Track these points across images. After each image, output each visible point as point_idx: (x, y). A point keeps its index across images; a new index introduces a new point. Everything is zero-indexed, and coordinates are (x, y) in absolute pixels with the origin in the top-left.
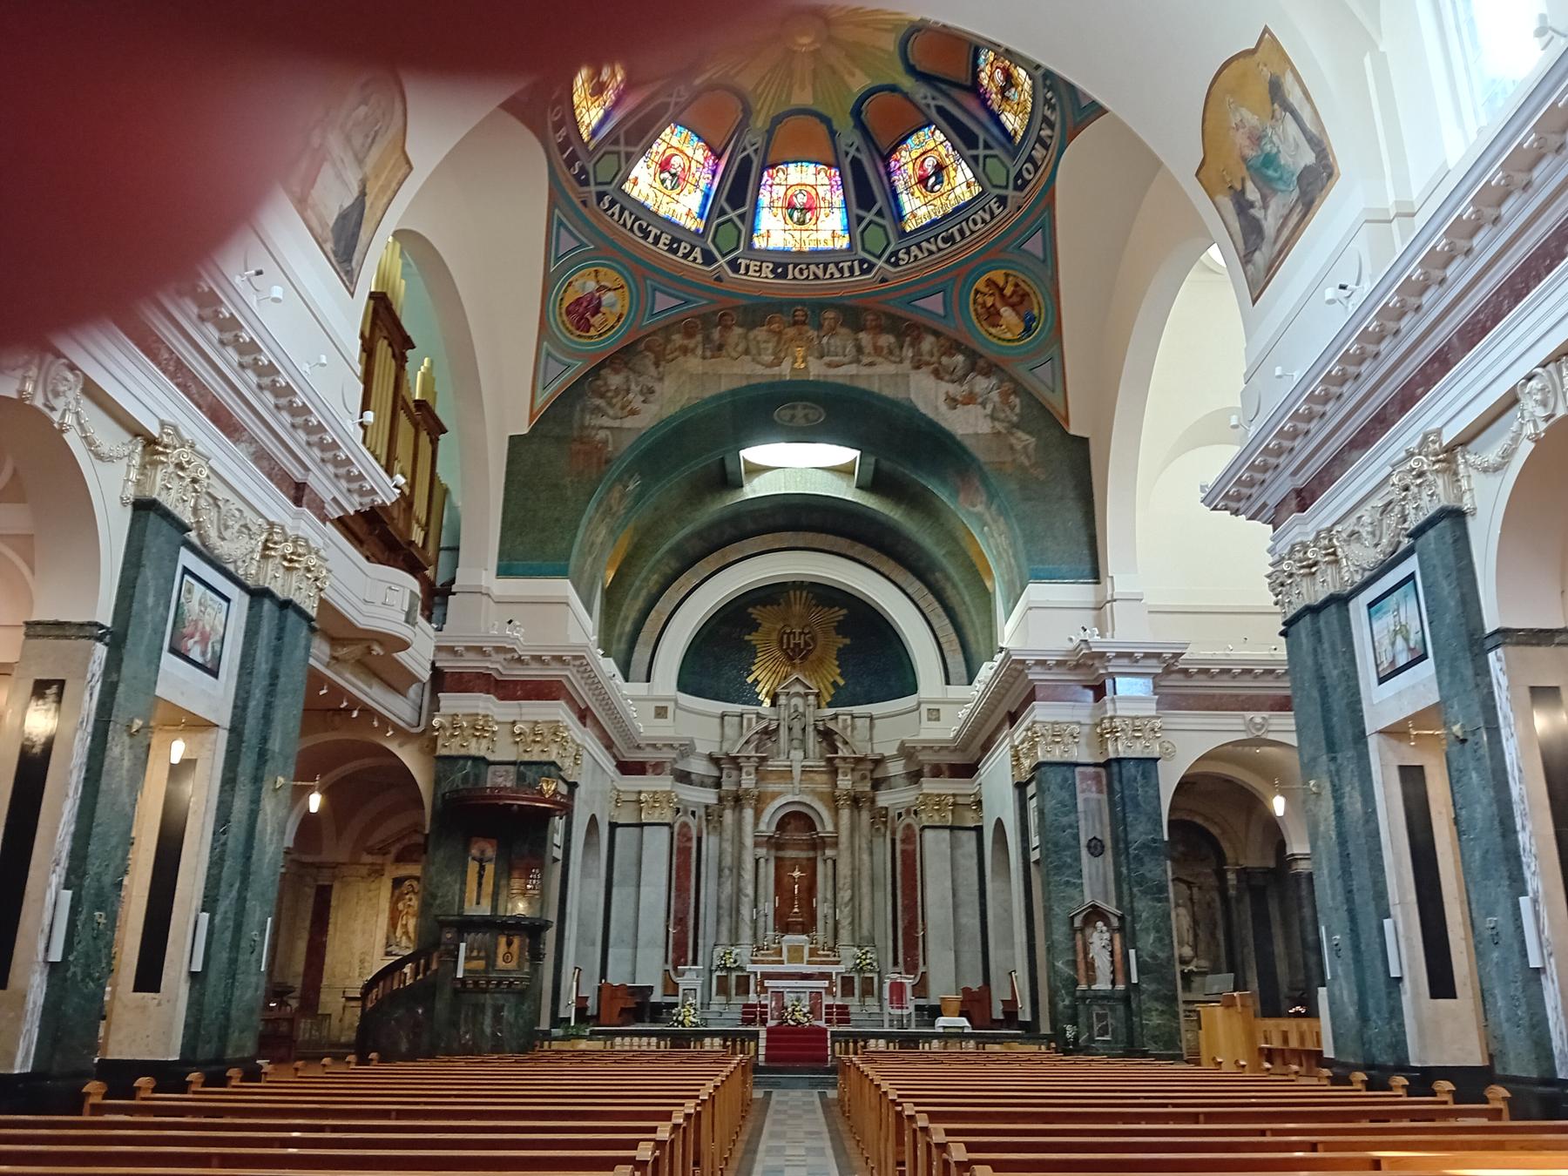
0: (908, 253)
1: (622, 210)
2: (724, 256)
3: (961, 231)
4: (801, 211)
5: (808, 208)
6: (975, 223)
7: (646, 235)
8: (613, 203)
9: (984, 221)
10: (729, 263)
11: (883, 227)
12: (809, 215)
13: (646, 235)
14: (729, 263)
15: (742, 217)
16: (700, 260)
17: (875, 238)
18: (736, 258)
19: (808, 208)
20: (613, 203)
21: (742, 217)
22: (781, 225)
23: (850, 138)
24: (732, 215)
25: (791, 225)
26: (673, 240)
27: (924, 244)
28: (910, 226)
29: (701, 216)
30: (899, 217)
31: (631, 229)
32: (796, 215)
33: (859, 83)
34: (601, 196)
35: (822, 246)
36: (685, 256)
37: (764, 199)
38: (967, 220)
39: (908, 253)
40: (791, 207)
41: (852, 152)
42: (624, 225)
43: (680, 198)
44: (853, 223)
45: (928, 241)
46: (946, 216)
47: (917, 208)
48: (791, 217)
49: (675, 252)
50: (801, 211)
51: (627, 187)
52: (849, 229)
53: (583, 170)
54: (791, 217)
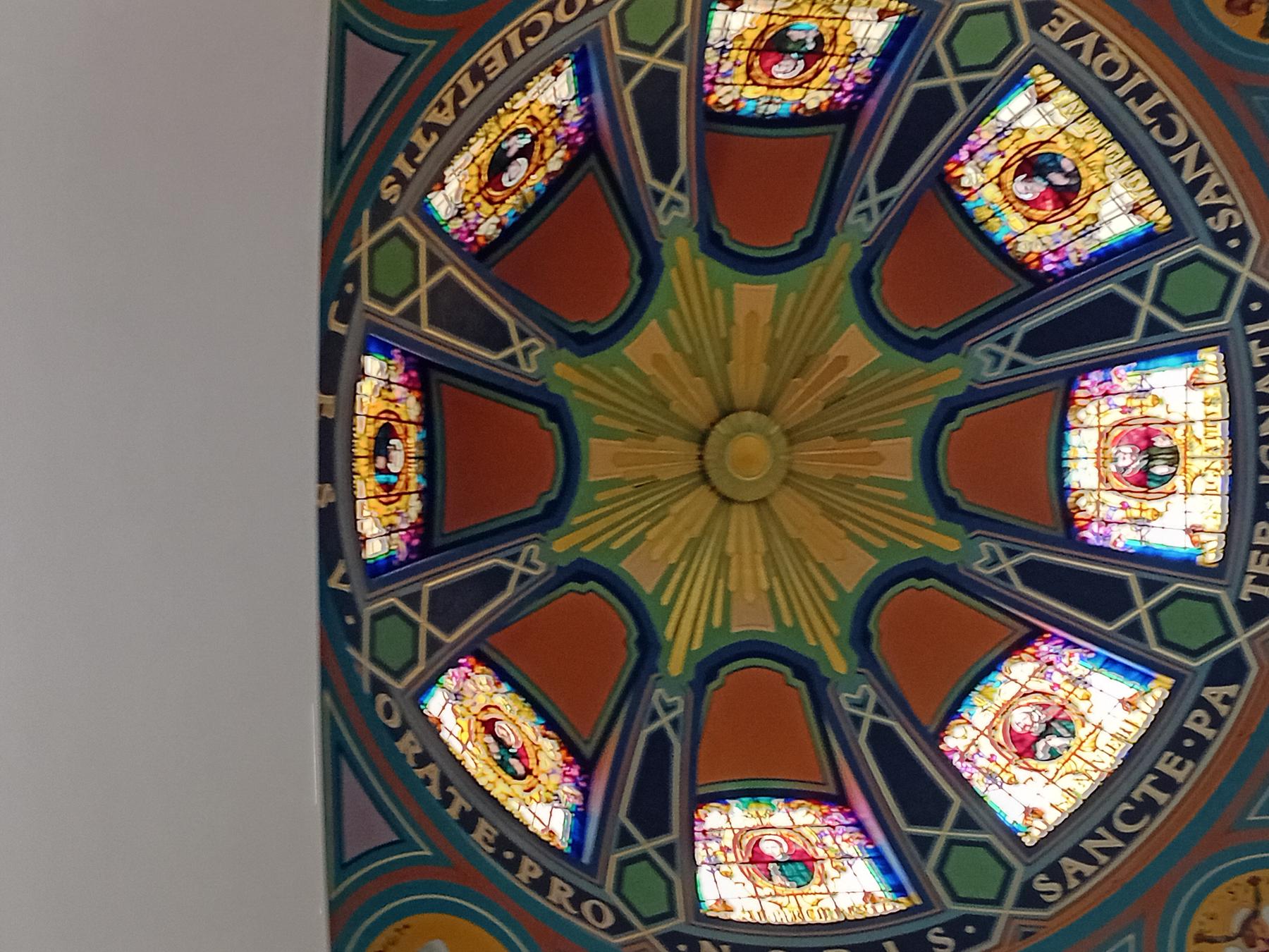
0: (1212, 211)
1: (1078, 853)
2: (1229, 635)
3: (1143, 93)
4: (1152, 462)
5: (1146, 443)
6: (1110, 67)
7: (1148, 807)
8: (1055, 873)
9: (1100, 47)
10: (1248, 622)
11: (1166, 272)
12: (1160, 442)
13: (1148, 807)
14: (1248, 622)
15: (1150, 588)
16: (1231, 690)
17: (1194, 290)
18: (1239, 604)
19: (1146, 443)
20: (1055, 873)
21: (1150, 588)
22: (1176, 500)
23: (984, 361)
24: (1142, 608)
25: (1178, 482)
26: (1175, 746)
27: (1189, 176)
28: (1157, 212)
29: (1146, 679)
30: (1148, 241)
31: (1127, 838)
32: (1161, 469)
33: (858, 348)
34: (1029, 897)
35: (1219, 410)
36: (1217, 722)
37: (1125, 538)
38: (1113, 86)
39: (1212, 211)
40: (1144, 480)
41: (1010, 353)
42: (1112, 852)
43: (1094, 718)
44: (1162, 345)
45: (1179, 167)
46: (1117, 137)
47: (1118, 208)
48: (1164, 479)
49: (1202, 743)
50: (1152, 462)
51: (1037, 830)
52: (1187, 350)
53: (953, 928)
54: (1164, 479)
